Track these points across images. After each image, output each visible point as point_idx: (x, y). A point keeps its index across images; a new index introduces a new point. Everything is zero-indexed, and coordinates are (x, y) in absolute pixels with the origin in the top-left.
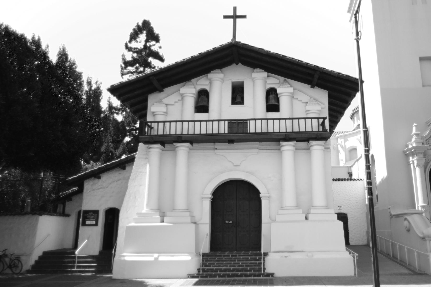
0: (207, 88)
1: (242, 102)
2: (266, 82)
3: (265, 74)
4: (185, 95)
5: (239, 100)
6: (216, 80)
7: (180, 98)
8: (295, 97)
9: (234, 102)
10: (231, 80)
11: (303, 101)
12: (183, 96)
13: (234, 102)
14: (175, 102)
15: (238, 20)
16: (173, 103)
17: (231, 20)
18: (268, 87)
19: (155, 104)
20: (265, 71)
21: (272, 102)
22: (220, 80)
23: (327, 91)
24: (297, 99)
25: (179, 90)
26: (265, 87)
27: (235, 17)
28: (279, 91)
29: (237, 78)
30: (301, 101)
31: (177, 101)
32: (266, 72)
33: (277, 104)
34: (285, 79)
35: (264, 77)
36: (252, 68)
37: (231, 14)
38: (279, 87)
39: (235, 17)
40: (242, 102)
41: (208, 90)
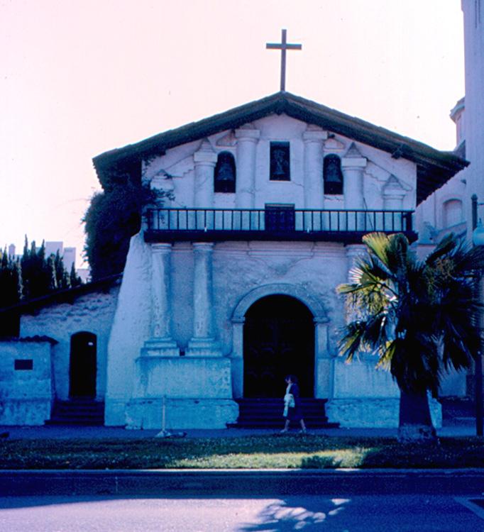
0: (232, 150)
1: (285, 176)
2: (324, 145)
4: (202, 163)
5: (280, 172)
7: (192, 168)
9: (274, 176)
12: (196, 165)
13: (274, 176)
14: (185, 173)
15: (288, 52)
16: (181, 175)
17: (279, 52)
19: (156, 177)
21: (334, 178)
22: (253, 140)
25: (193, 155)
27: (284, 47)
28: (344, 163)
31: (186, 171)
33: (339, 181)
34: (353, 146)
35: (324, 140)
37: (279, 41)
38: (345, 157)
39: (284, 47)
40: (285, 176)
41: (235, 157)
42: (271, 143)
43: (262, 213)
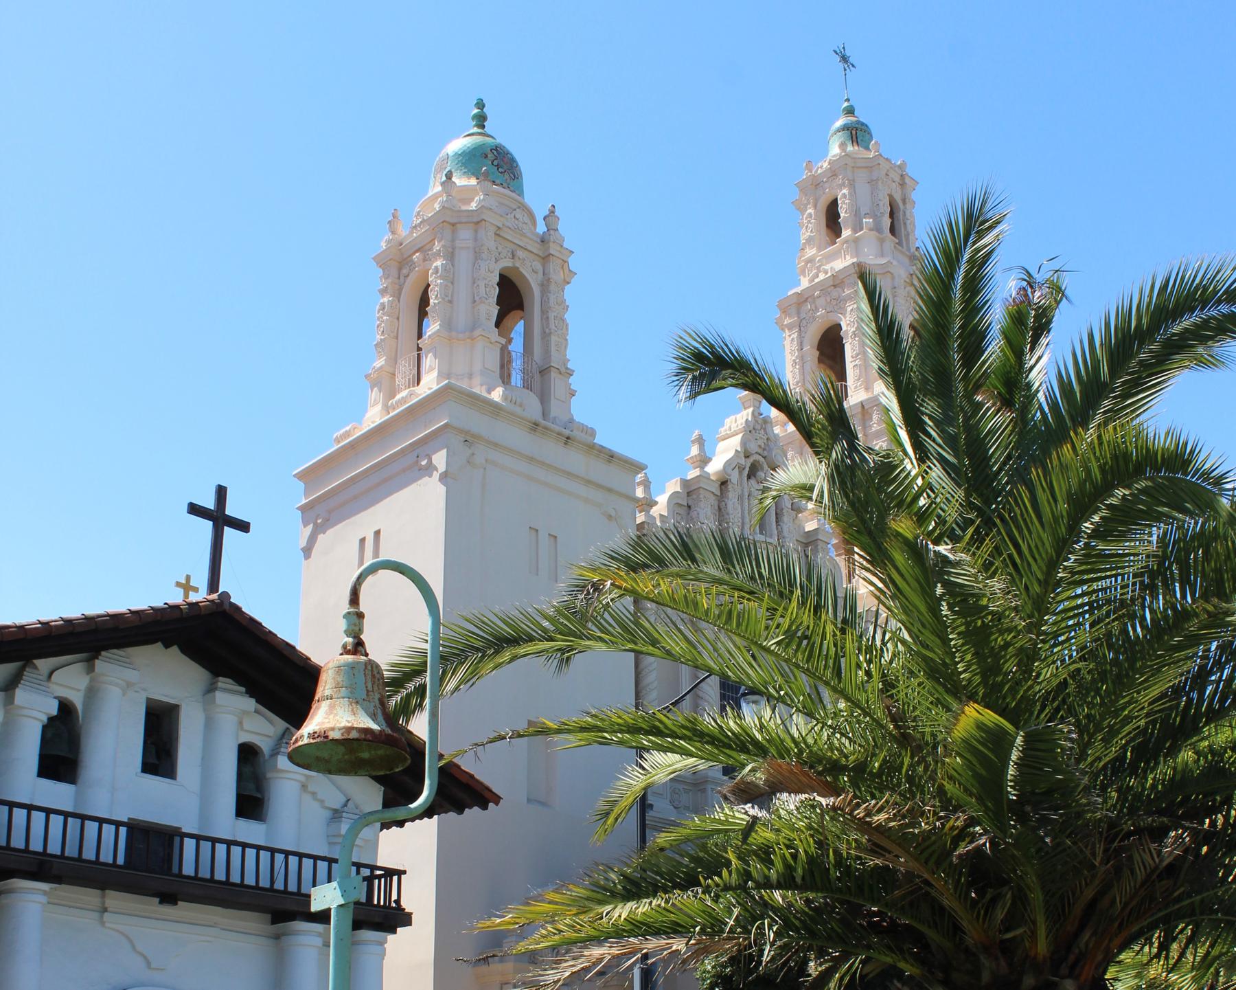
2: (241, 723)
3: (250, 704)
6: (117, 685)
8: (310, 788)
10: (144, 690)
11: (327, 804)
18: (245, 738)
20: (247, 692)
21: (250, 790)
23: (383, 788)
24: (314, 794)
26: (237, 739)
29: (165, 693)
30: (322, 801)
32: (251, 697)
34: (288, 728)
35: (245, 713)
36: (207, 672)
42: (149, 701)
43: (123, 830)
